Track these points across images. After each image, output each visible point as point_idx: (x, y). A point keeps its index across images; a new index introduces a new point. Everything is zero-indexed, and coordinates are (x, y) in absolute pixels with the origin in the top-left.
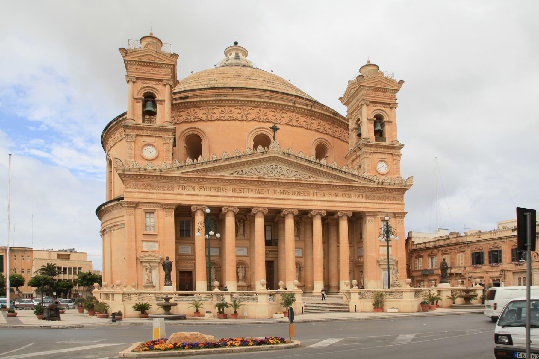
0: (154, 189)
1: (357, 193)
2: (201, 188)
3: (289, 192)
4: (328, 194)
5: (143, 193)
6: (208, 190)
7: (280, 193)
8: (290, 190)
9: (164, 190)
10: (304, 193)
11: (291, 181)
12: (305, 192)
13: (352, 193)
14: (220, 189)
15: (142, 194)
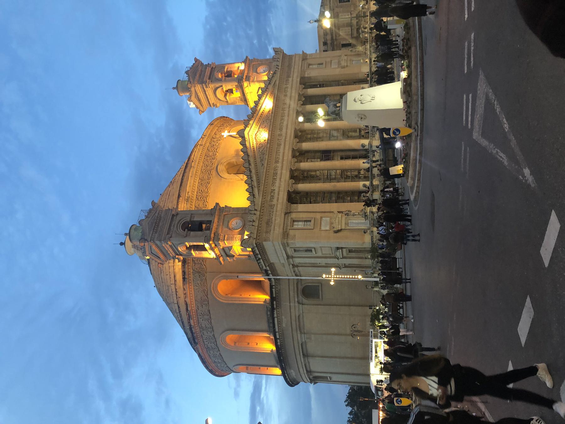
0: (272, 219)
1: (285, 83)
3: (281, 126)
5: (274, 227)
6: (275, 180)
9: (273, 212)
10: (283, 116)
11: (272, 122)
13: (284, 86)
14: (275, 172)
15: (275, 228)
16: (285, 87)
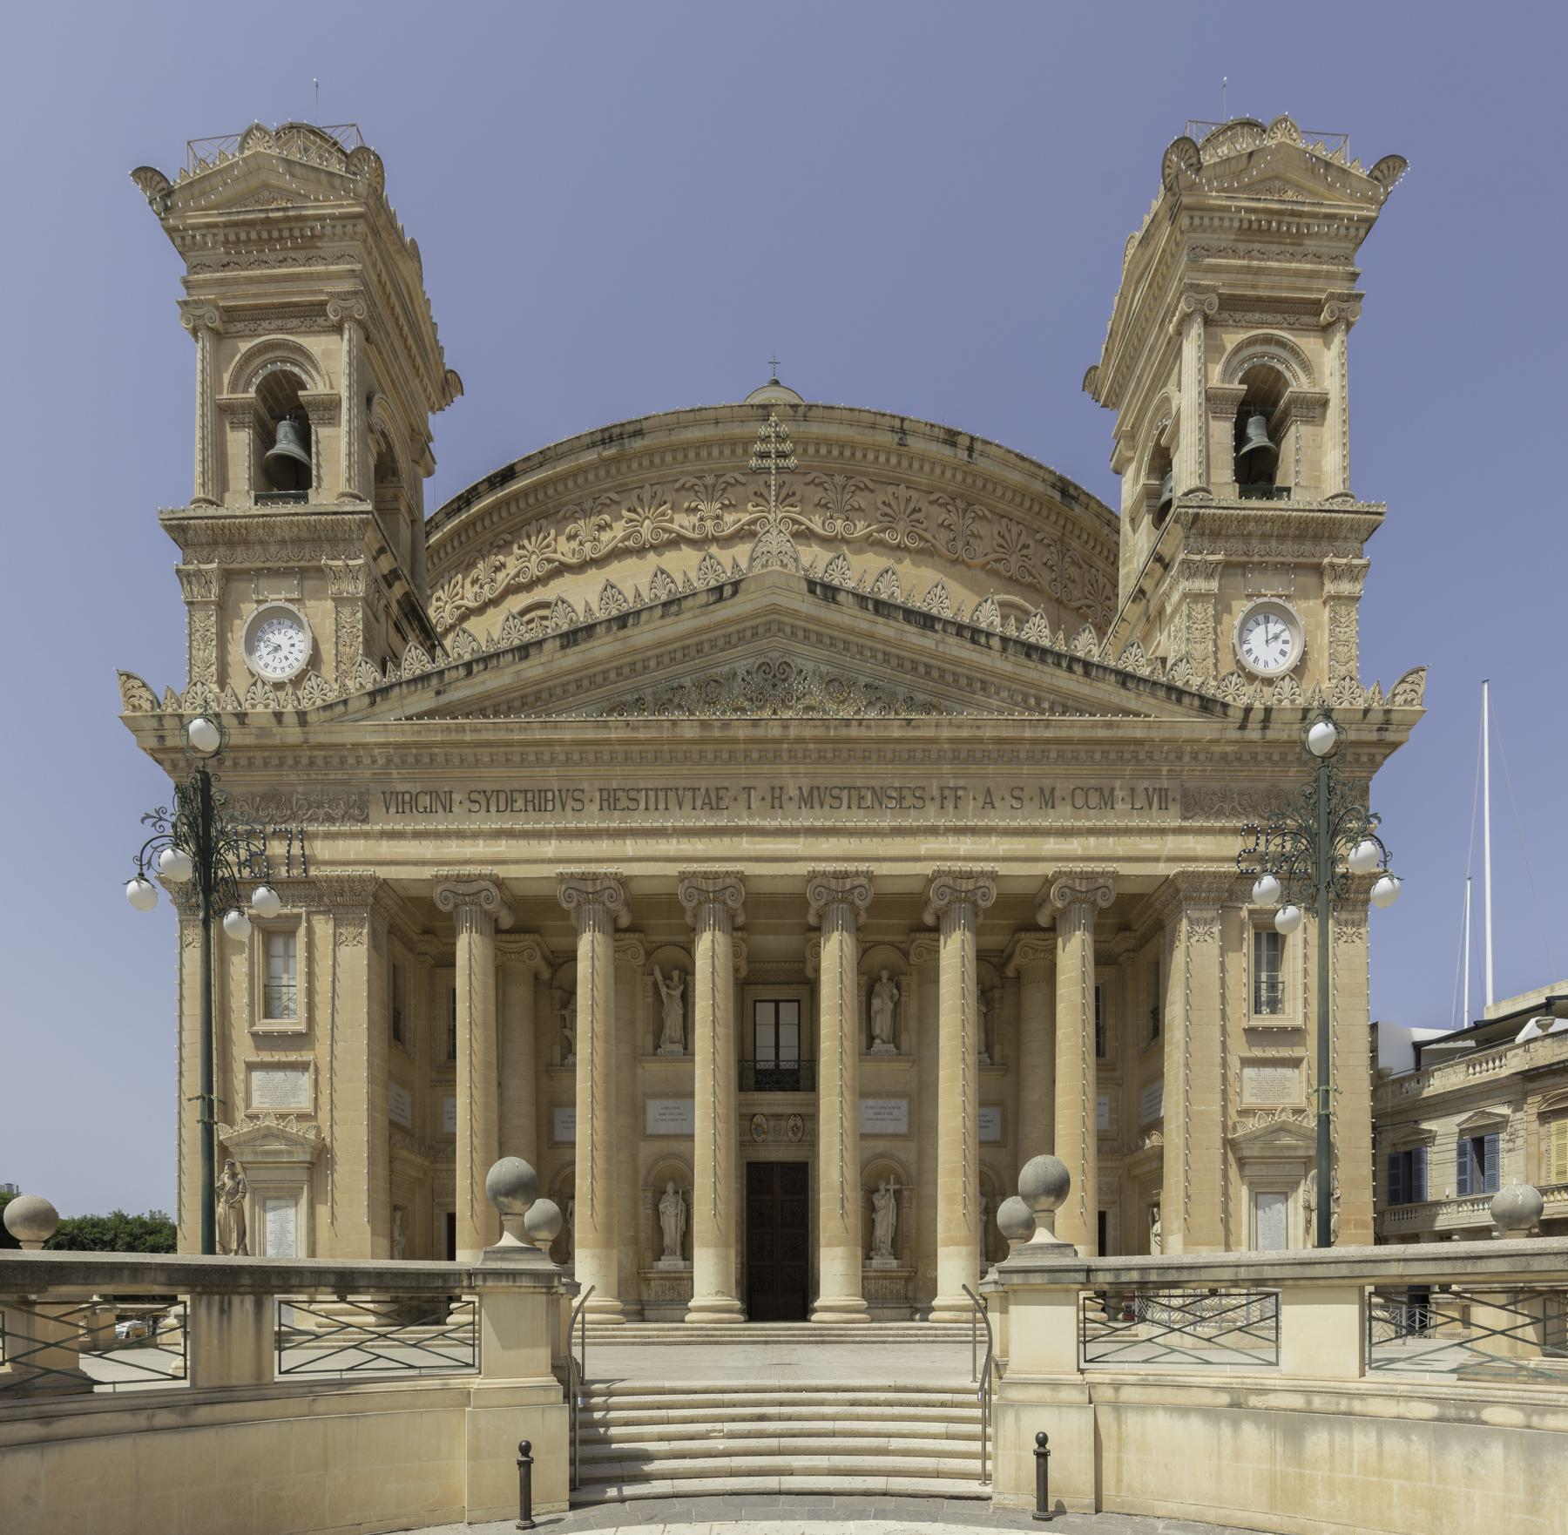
2: (474, 796)
3: (835, 792)
4: (1008, 797)
6: (502, 808)
7: (797, 799)
8: (839, 782)
10: (902, 798)
12: (905, 792)
13: (1118, 784)
14: (550, 796)
16: (1112, 790)
